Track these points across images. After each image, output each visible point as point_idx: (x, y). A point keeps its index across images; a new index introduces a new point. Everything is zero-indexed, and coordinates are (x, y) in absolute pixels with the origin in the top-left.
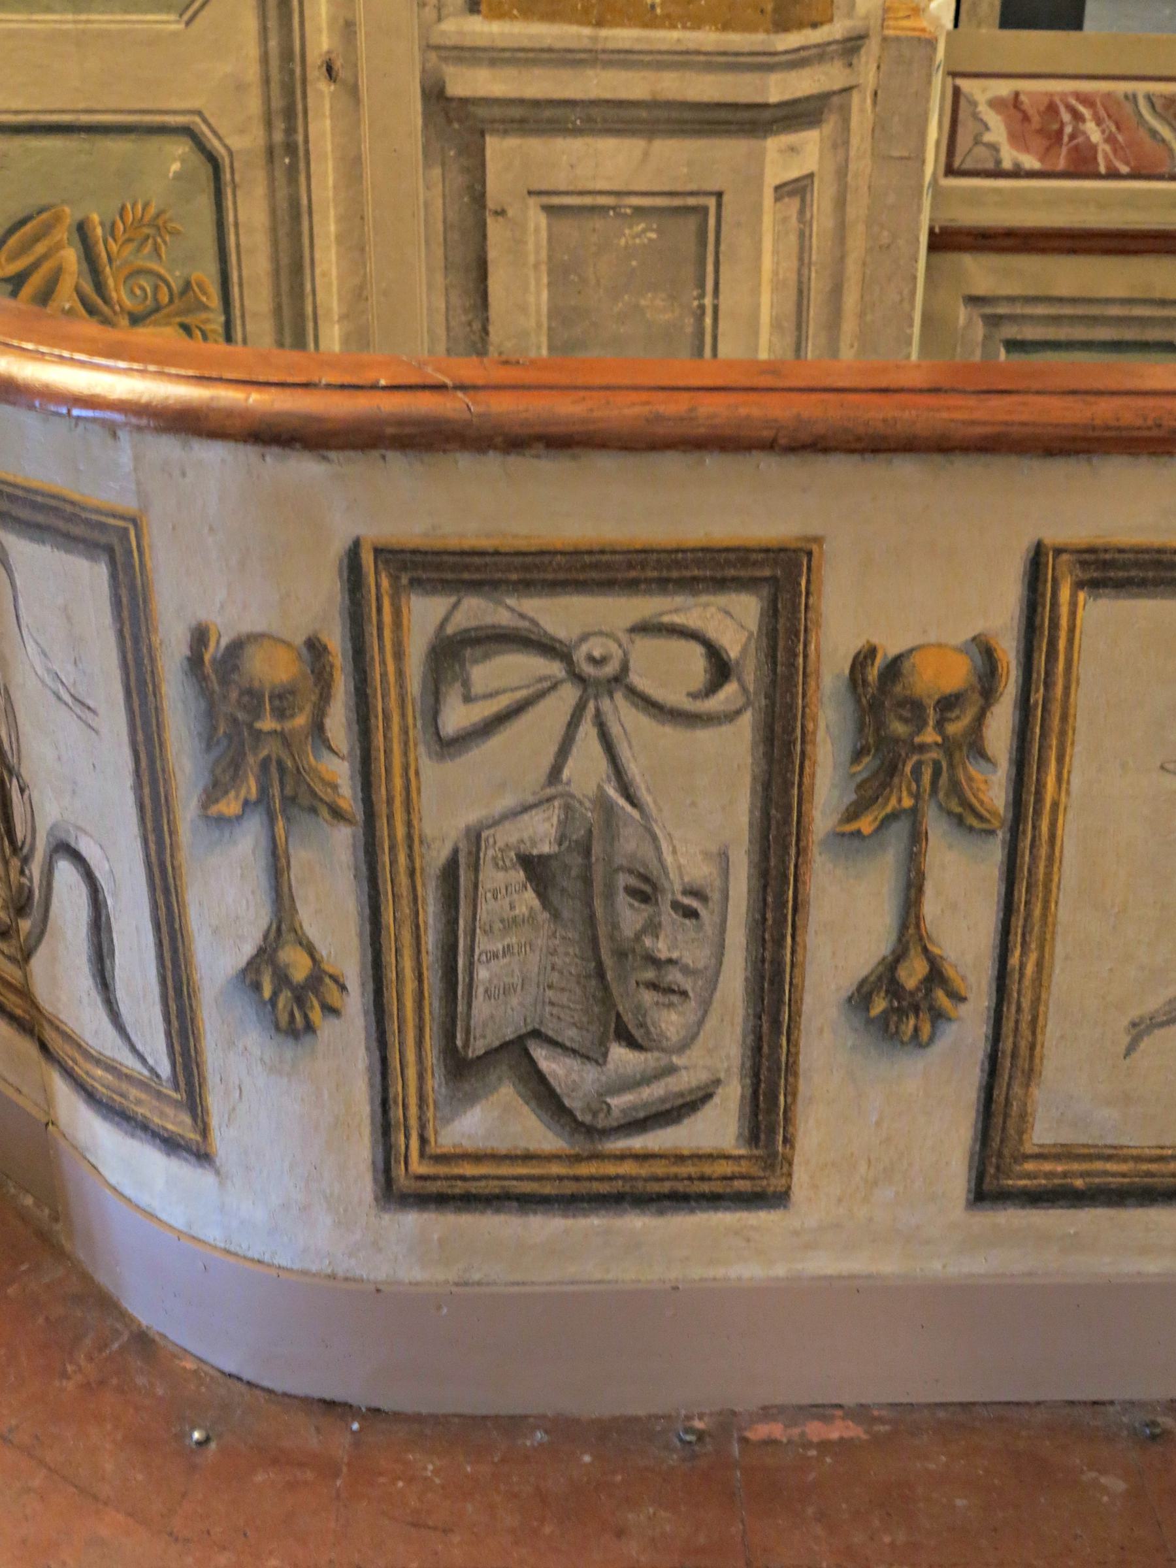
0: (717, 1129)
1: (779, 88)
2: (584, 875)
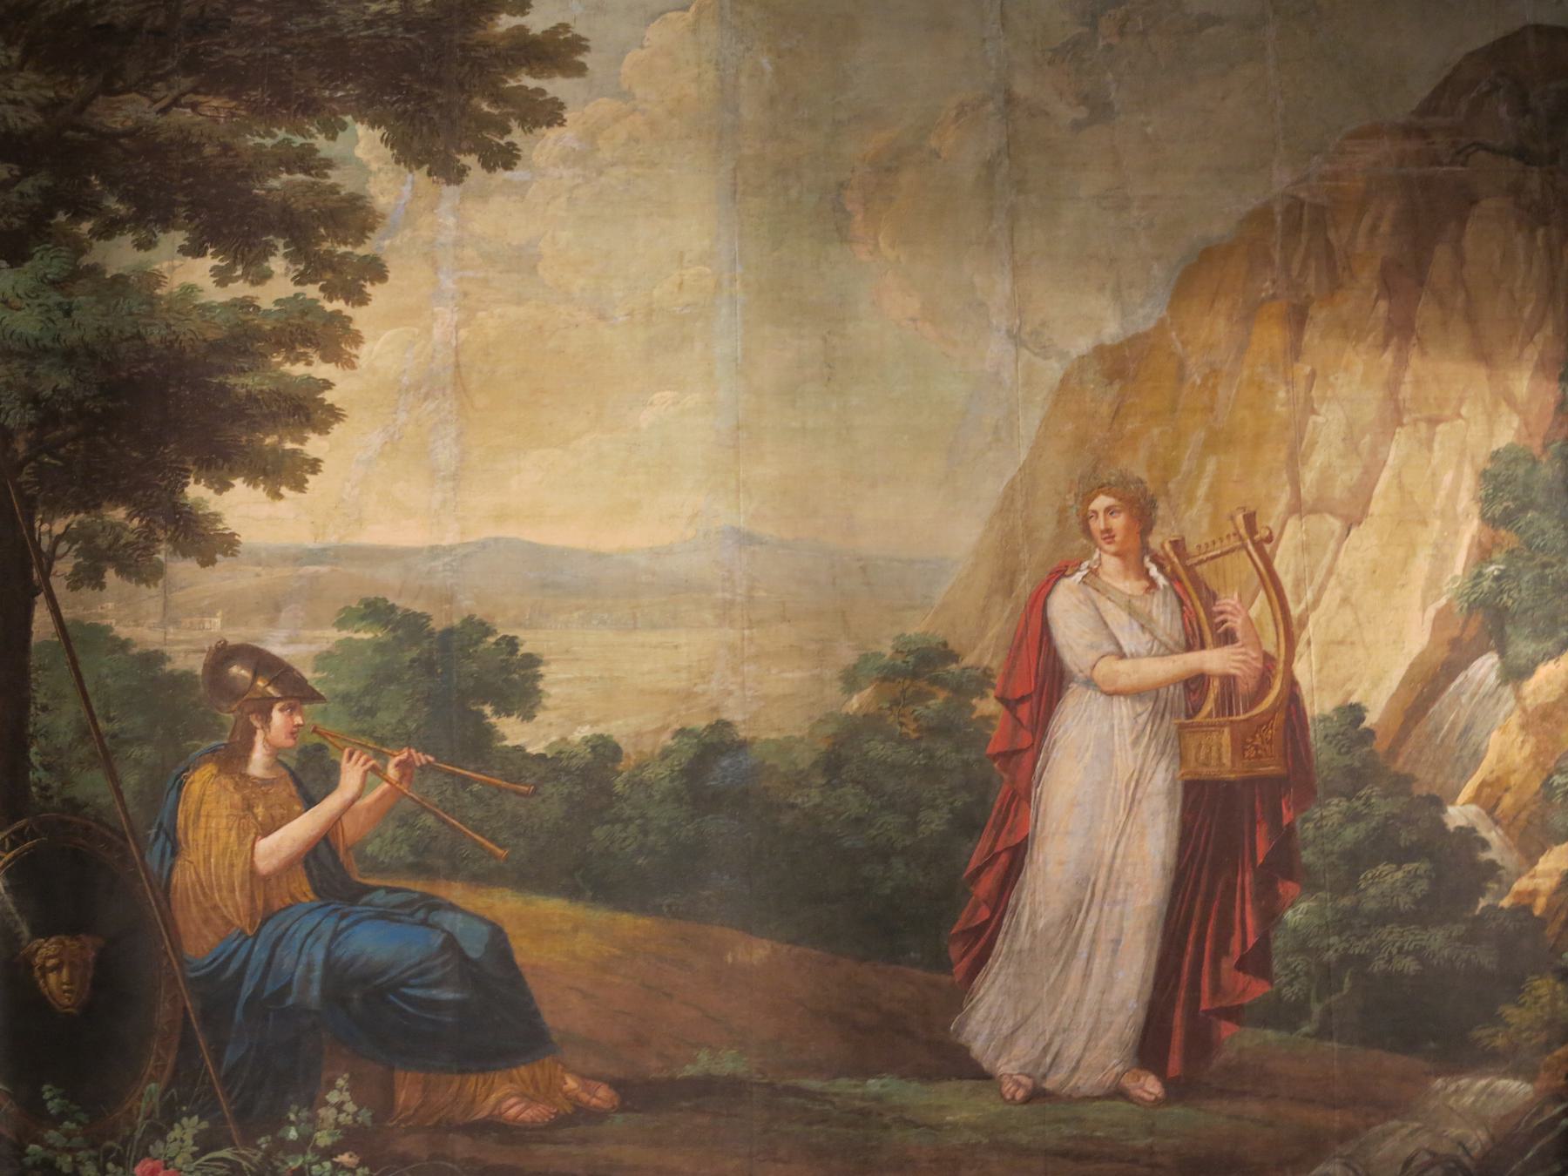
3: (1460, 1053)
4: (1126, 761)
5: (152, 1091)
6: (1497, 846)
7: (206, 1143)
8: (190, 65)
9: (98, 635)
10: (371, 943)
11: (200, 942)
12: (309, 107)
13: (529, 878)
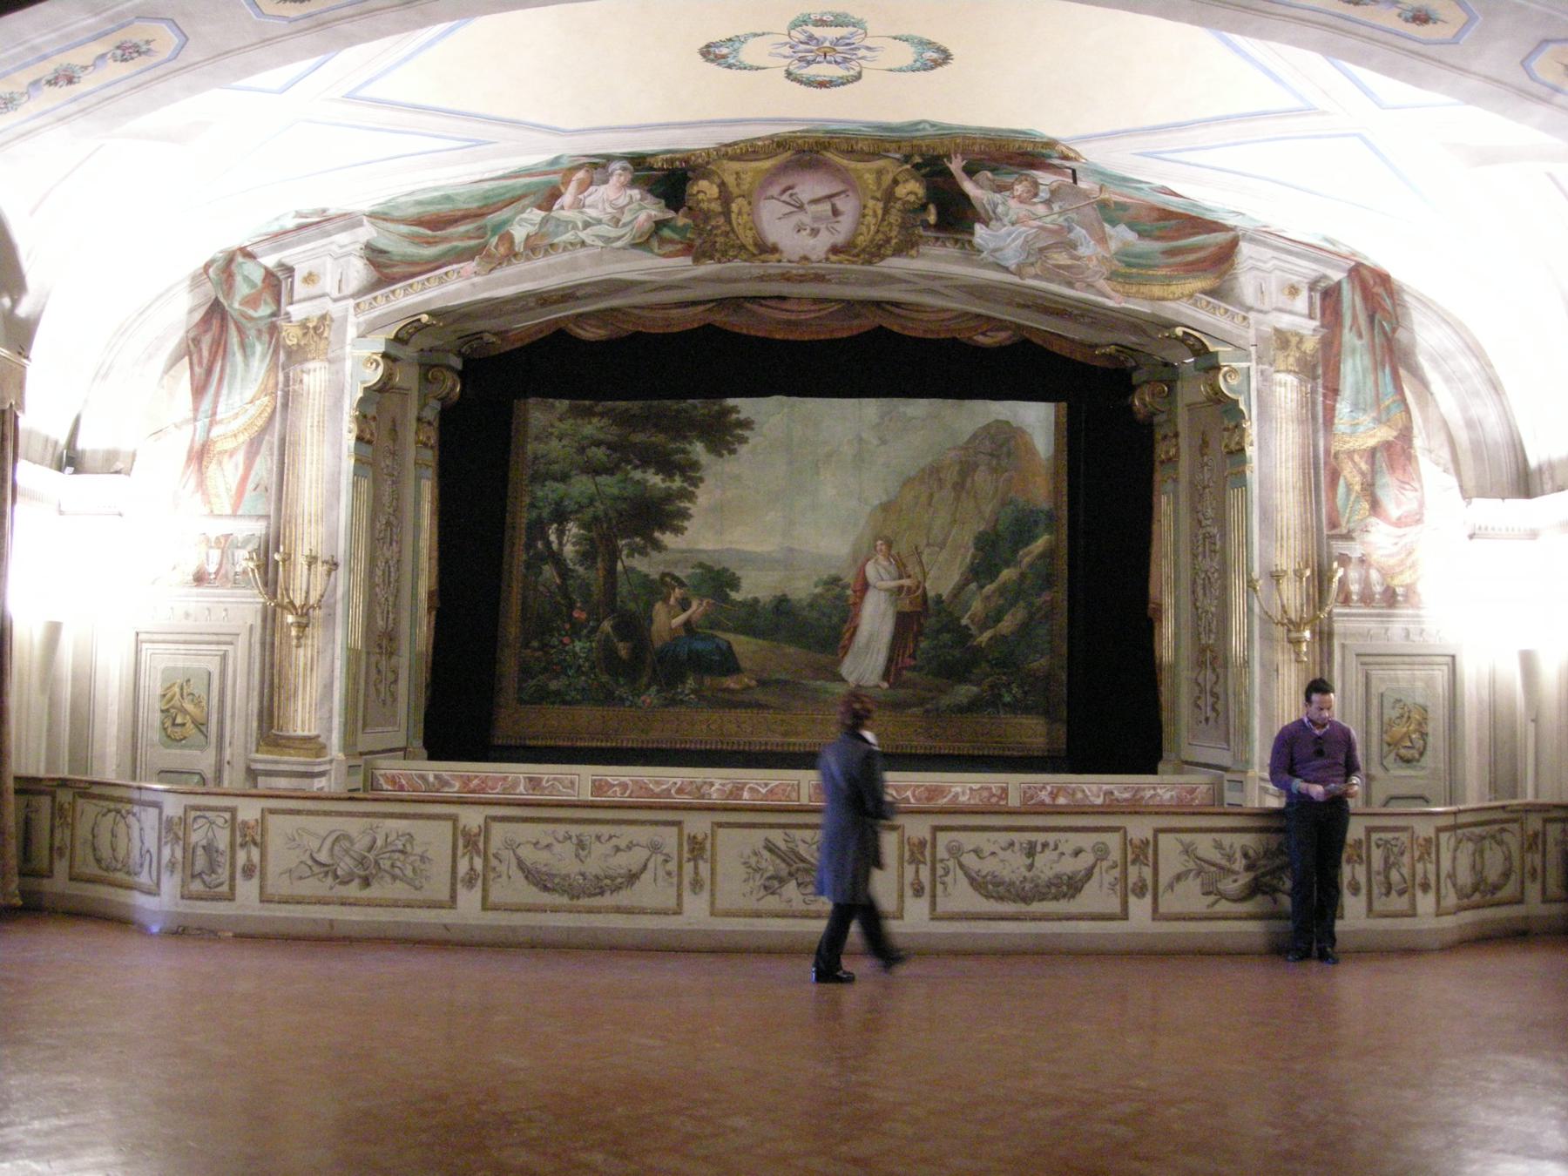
0: (225, 888)
1: (317, 769)
2: (209, 849)
3: (963, 680)
4: (883, 606)
5: (645, 680)
6: (974, 630)
7: (658, 692)
8: (655, 425)
9: (633, 570)
10: (699, 646)
11: (658, 644)
12: (685, 438)
13: (736, 631)
